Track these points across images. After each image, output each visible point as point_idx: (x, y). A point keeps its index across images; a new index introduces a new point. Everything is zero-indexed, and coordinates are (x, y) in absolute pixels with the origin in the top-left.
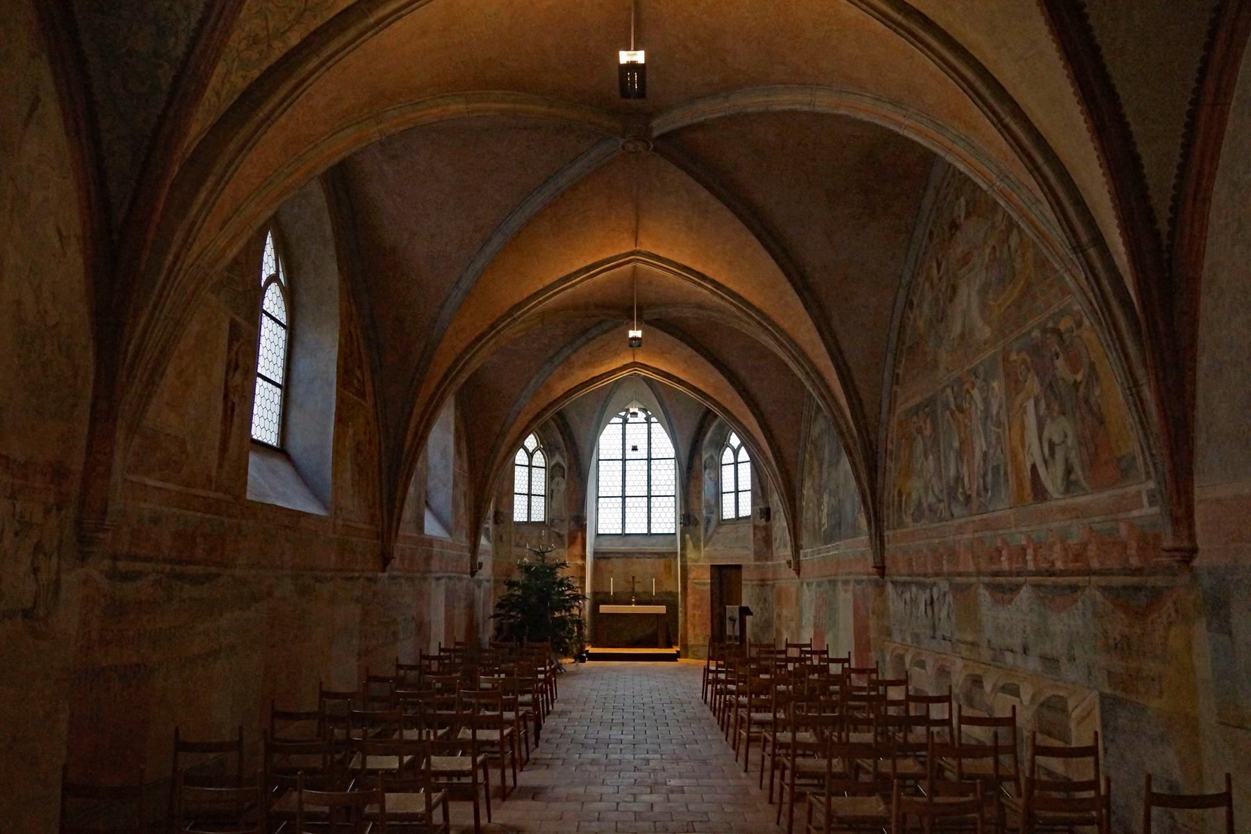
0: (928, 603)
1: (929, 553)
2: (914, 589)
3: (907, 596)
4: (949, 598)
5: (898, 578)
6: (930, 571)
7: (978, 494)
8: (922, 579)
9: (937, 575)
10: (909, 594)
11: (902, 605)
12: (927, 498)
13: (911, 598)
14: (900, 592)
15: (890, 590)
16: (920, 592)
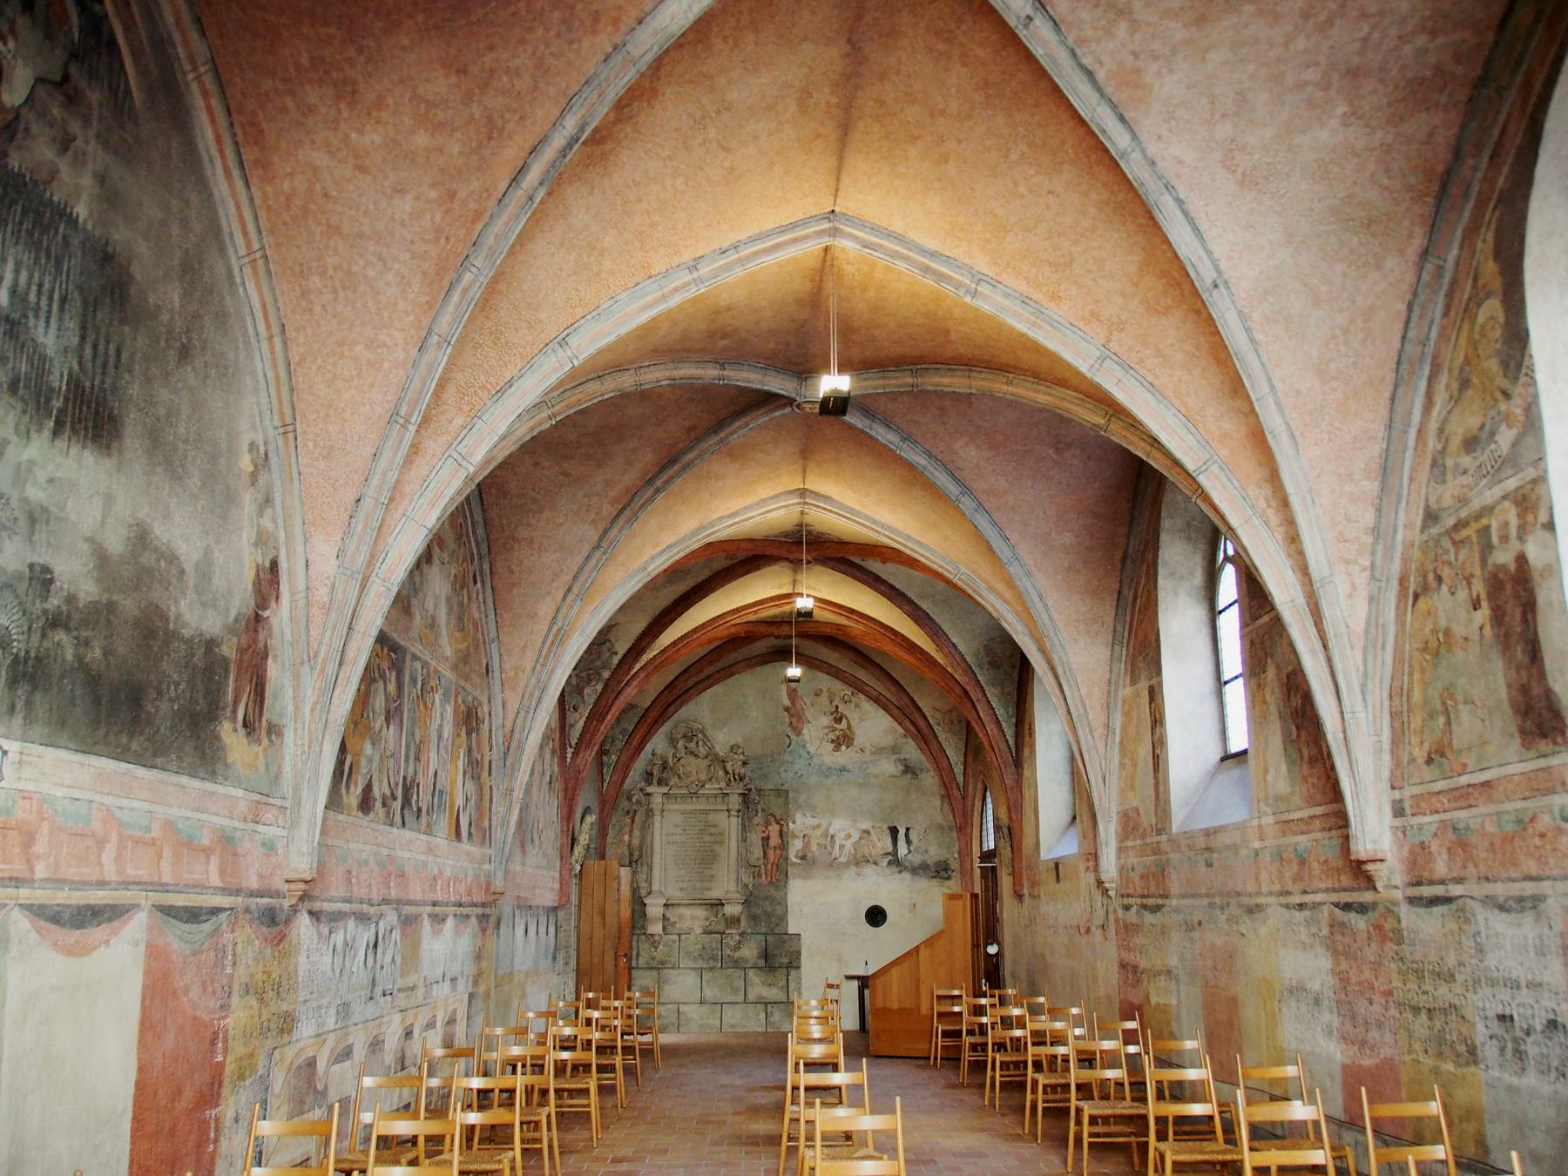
0: (371, 945)
1: (376, 869)
2: (351, 924)
3: (339, 938)
4: (396, 934)
5: (326, 906)
6: (376, 897)
7: (428, 812)
8: (365, 908)
9: (386, 901)
10: (342, 932)
11: (327, 959)
12: (380, 785)
13: (345, 940)
14: (325, 931)
15: (303, 930)
16: (361, 927)
